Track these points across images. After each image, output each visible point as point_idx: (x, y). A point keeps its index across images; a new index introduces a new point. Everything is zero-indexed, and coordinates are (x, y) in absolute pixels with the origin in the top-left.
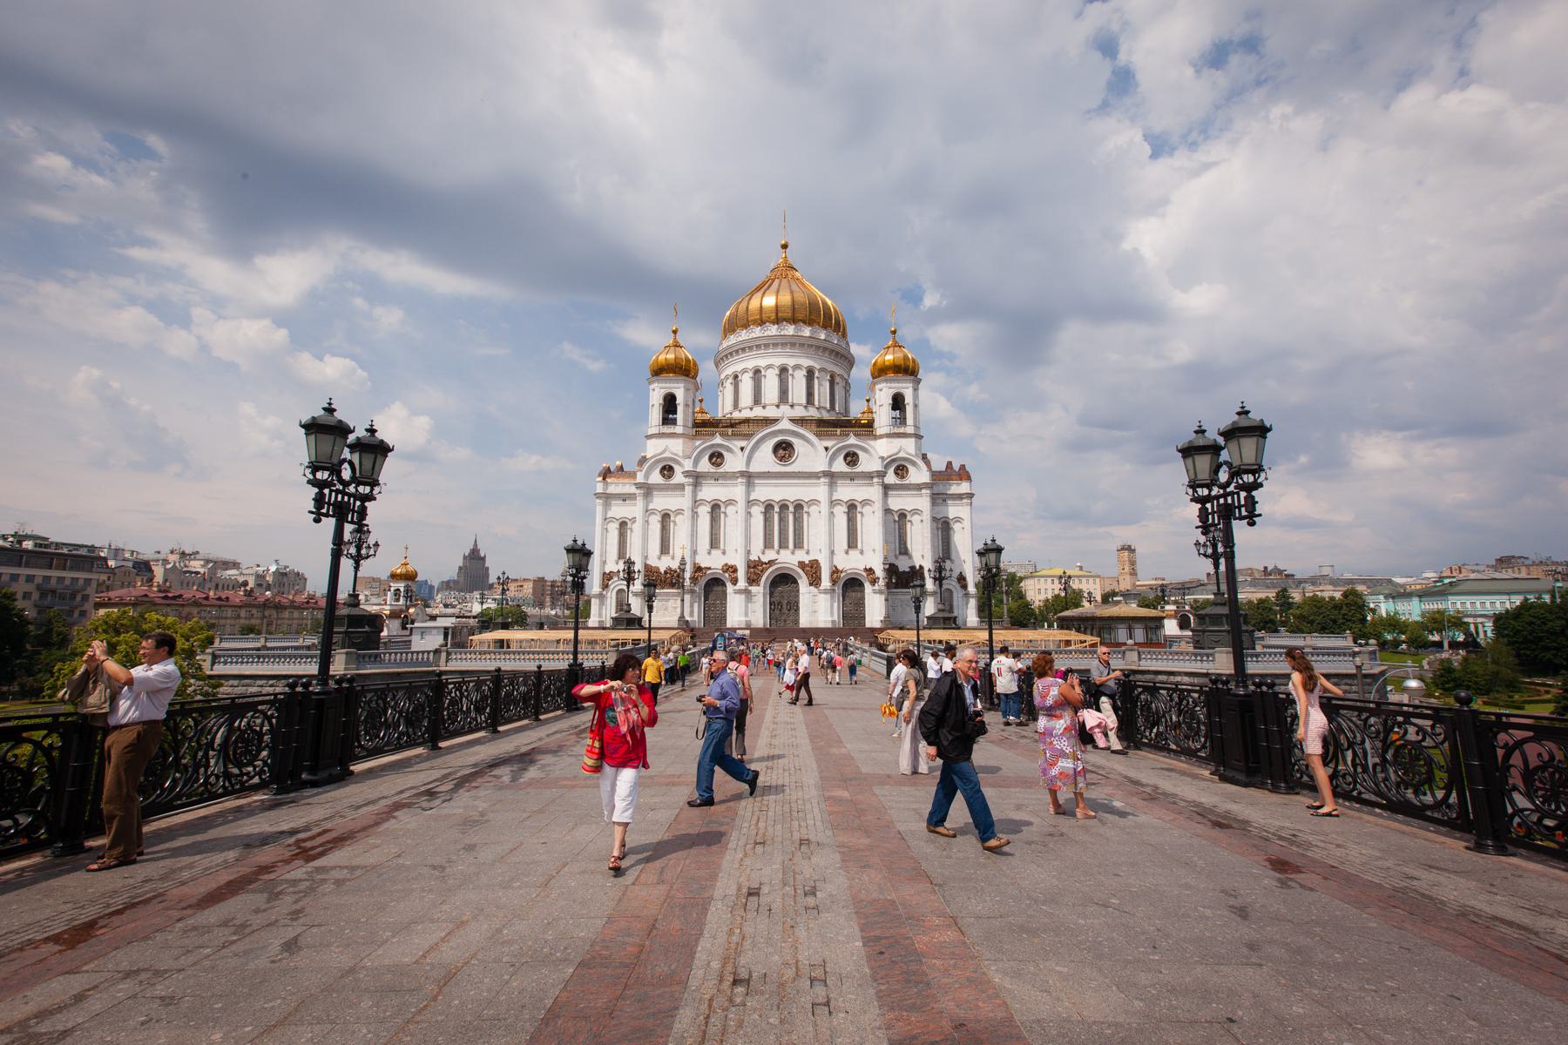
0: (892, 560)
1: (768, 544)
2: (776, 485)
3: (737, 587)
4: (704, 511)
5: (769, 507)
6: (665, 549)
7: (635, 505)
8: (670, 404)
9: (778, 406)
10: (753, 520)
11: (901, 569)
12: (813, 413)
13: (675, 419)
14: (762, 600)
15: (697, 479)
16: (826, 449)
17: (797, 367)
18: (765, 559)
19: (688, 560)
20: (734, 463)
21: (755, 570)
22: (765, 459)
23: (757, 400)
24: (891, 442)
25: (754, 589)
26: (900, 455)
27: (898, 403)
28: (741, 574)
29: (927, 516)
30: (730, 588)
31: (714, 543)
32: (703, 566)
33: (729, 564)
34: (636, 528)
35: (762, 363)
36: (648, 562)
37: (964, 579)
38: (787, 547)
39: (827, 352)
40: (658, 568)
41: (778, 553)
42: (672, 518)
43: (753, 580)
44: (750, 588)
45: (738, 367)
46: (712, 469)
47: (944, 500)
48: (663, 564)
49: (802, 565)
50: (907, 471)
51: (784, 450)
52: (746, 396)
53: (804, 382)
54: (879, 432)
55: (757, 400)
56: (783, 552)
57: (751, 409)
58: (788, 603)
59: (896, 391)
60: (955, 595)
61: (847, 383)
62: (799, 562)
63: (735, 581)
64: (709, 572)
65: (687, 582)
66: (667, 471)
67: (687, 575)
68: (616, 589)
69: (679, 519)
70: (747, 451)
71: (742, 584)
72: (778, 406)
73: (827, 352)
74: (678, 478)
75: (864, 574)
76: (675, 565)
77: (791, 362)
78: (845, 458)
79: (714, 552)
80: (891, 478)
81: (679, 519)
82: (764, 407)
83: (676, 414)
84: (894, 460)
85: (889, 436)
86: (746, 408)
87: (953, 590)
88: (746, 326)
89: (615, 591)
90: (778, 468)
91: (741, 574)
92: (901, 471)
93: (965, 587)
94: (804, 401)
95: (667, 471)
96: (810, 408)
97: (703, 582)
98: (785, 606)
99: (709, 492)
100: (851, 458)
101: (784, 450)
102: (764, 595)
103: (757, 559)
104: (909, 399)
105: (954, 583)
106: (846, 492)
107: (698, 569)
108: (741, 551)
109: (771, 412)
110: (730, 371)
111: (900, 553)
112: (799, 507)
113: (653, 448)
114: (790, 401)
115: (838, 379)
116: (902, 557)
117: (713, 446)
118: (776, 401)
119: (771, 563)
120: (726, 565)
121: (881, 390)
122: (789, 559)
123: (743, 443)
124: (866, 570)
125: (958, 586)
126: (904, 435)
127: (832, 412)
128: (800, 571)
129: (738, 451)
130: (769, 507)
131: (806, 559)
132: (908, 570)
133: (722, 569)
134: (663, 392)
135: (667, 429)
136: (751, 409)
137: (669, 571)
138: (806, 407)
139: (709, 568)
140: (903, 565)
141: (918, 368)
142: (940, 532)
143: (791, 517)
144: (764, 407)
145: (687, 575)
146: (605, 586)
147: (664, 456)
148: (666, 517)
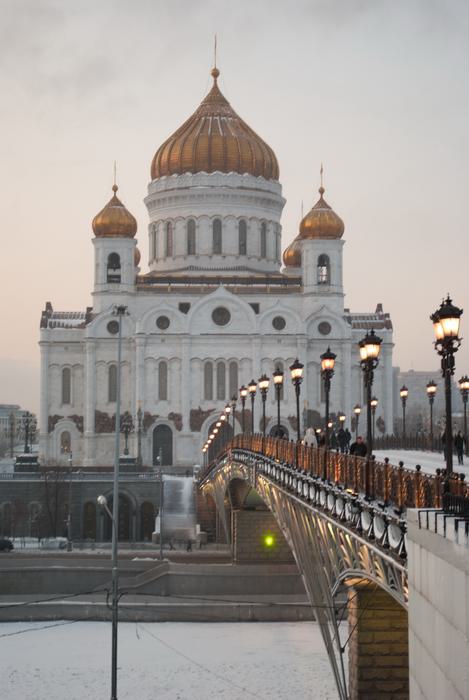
0: (313, 407)
1: (208, 396)
3: (182, 433)
4: (153, 367)
8: (114, 261)
9: (211, 257)
12: (243, 261)
13: (119, 277)
15: (148, 338)
16: (256, 307)
18: (205, 408)
20: (179, 323)
21: (198, 418)
22: (209, 325)
23: (191, 249)
24: (316, 301)
25: (196, 434)
26: (325, 312)
27: (323, 261)
30: (176, 434)
31: (163, 395)
33: (175, 412)
35: (196, 213)
36: (98, 408)
37: (383, 423)
41: (215, 403)
44: (194, 433)
48: (111, 410)
50: (330, 328)
51: (221, 316)
52: (180, 245)
53: (236, 233)
54: (306, 290)
55: (191, 249)
57: (185, 258)
59: (320, 253)
61: (278, 227)
63: (179, 427)
64: (158, 420)
68: (61, 432)
75: (287, 421)
79: (162, 403)
80: (316, 334)
82: (197, 258)
83: (119, 267)
86: (179, 256)
89: (59, 436)
90: (218, 329)
91: (186, 420)
92: (324, 328)
96: (243, 258)
97: (152, 428)
99: (159, 351)
100: (279, 323)
101: (221, 316)
103: (197, 408)
104: (333, 262)
106: (275, 352)
107: (149, 419)
110: (165, 216)
114: (223, 251)
115: (270, 227)
117: (158, 311)
118: (210, 251)
119: (210, 411)
120: (172, 414)
121: (307, 251)
123: (185, 299)
124: (289, 418)
127: (264, 261)
129: (178, 313)
135: (112, 286)
136: (185, 258)
138: (237, 258)
139: (157, 416)
143: (227, 374)
144: (197, 258)
146: (51, 429)
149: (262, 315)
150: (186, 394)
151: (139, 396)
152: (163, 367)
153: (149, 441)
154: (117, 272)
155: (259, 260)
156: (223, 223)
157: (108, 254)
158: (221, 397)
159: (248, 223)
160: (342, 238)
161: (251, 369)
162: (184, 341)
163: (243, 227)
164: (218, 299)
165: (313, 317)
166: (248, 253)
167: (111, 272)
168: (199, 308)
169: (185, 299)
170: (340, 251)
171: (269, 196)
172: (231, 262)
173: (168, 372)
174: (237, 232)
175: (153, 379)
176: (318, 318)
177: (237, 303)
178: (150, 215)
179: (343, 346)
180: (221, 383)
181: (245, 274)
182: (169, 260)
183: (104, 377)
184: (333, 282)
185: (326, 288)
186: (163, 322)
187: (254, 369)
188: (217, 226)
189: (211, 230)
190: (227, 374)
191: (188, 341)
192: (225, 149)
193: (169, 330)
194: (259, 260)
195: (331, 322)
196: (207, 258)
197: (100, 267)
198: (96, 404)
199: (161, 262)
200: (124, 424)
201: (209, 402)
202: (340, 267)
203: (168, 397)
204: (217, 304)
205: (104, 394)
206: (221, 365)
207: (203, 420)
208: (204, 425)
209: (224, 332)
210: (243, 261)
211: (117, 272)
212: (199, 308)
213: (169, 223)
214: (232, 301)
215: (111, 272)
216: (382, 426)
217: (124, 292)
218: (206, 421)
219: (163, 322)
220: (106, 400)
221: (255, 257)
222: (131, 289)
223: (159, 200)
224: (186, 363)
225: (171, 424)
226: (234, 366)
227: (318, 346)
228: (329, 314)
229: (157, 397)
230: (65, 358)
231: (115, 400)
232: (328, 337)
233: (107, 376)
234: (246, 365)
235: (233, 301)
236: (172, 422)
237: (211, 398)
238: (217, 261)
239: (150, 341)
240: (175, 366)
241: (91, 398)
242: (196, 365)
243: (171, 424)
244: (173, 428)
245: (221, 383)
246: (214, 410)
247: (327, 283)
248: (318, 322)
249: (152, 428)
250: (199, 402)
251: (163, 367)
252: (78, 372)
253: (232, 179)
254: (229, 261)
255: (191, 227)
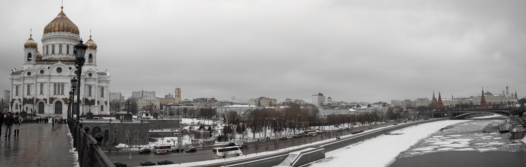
0: (86, 97)
1: (55, 94)
2: (57, 78)
4: (39, 85)
5: (55, 84)
6: (28, 94)
7: (21, 81)
8: (30, 55)
9: (59, 55)
10: (51, 88)
11: (89, 100)
12: (68, 56)
14: (53, 107)
15: (37, 76)
17: (64, 44)
18: (54, 97)
19: (35, 97)
20: (47, 73)
21: (52, 100)
22: (54, 72)
23: (53, 52)
24: (88, 67)
26: (91, 70)
28: (48, 101)
29: (97, 86)
31: (41, 93)
32: (38, 99)
34: (21, 87)
35: (55, 43)
36: (24, 97)
37: (107, 102)
38: (60, 94)
39: (73, 40)
40: (27, 98)
41: (57, 96)
42: (30, 86)
43: (51, 102)
44: (51, 104)
45: (49, 43)
46: (41, 74)
47: (103, 82)
48: (28, 97)
49: (63, 99)
51: (59, 70)
55: (53, 52)
56: (58, 96)
57: (51, 55)
58: (60, 108)
60: (104, 107)
62: (62, 98)
63: (46, 103)
64: (40, 100)
65: (35, 103)
66: (29, 74)
67: (35, 101)
69: (32, 86)
70: (50, 68)
71: (48, 103)
72: (59, 55)
73: (73, 40)
74: (32, 75)
76: (31, 98)
77: (63, 43)
78: (75, 73)
79: (41, 95)
80: (88, 76)
81: (32, 86)
84: (89, 72)
85: (87, 65)
87: (104, 105)
88: (51, 32)
89: (15, 105)
91: (48, 101)
92: (90, 75)
93: (106, 104)
94: (66, 53)
95: (29, 74)
96: (68, 55)
97: (38, 103)
98: (59, 109)
99: (40, 80)
101: (59, 70)
102: (54, 106)
104: (93, 56)
105: (104, 103)
107: (37, 100)
108: (48, 95)
109: (56, 57)
110: (46, 44)
111: (89, 96)
112: (63, 84)
113: (26, 67)
114: (62, 53)
116: (89, 97)
117: (41, 68)
118: (58, 53)
122: (60, 97)
123: (49, 66)
125: (105, 104)
126: (92, 65)
128: (63, 100)
130: (55, 84)
131: (64, 97)
132: (91, 100)
133: (43, 100)
134: (28, 52)
136: (51, 55)
137: (30, 99)
138: (66, 55)
139: (40, 99)
140: (90, 99)
141: (97, 46)
142: (101, 90)
143: (61, 87)
145: (35, 101)
147: (28, 69)
148: (29, 86)
149: (71, 70)
150: (48, 93)
151: (35, 93)
152: (42, 85)
153: (37, 106)
154: (31, 58)
155: (73, 56)
156: (62, 45)
157: (28, 53)
158: (59, 94)
159: (70, 46)
160: (97, 49)
161: (68, 86)
162: (48, 77)
163: (68, 46)
164: (58, 65)
165: (87, 71)
166: (69, 54)
167: (30, 58)
168: (52, 68)
169: (49, 66)
170: (96, 53)
171: (75, 38)
172: (64, 56)
173: (43, 86)
174: (66, 48)
175: (39, 88)
176: (89, 72)
177: (64, 66)
178: (43, 44)
179: (96, 80)
180: (59, 90)
181: (69, 59)
182: (47, 56)
183: (26, 88)
184: (93, 61)
185: (91, 63)
186: (42, 72)
187: (69, 85)
188: (61, 46)
189: (59, 47)
190: (61, 87)
191: (49, 77)
192: (63, 25)
193: (44, 74)
194: (73, 56)
195: (92, 73)
196: (57, 55)
197: (26, 57)
198: (23, 95)
199: (45, 56)
200: (31, 101)
201: (55, 95)
202: (95, 57)
203: (43, 94)
204: (58, 66)
205: (26, 93)
206: (59, 84)
207: (53, 100)
208: (53, 102)
209: (60, 75)
210: (68, 56)
211: (31, 58)
212: (52, 68)
213: (47, 46)
214: (63, 66)
215: (30, 58)
216: (106, 103)
217: (32, 64)
218: (54, 101)
219: (42, 72)
220: (27, 94)
221: (72, 55)
222: (35, 63)
223: (45, 40)
224: (48, 84)
225: (44, 102)
226: (63, 84)
227: (88, 80)
228: (91, 71)
229: (40, 94)
230: (16, 83)
231: (29, 95)
232: (91, 77)
233: (27, 88)
234: (66, 85)
235: (63, 66)
236: (44, 101)
237: (56, 94)
238: (61, 56)
239: (38, 77)
240: (45, 84)
241: (23, 94)
242: (52, 85)
243: (44, 102)
244: (44, 103)
245: (59, 90)
246: (57, 98)
247: (92, 61)
248: (88, 73)
249: (38, 103)
250: (52, 95)
251: (42, 85)
252: (20, 87)
253: (66, 34)
254: (64, 56)
255: (53, 46)
